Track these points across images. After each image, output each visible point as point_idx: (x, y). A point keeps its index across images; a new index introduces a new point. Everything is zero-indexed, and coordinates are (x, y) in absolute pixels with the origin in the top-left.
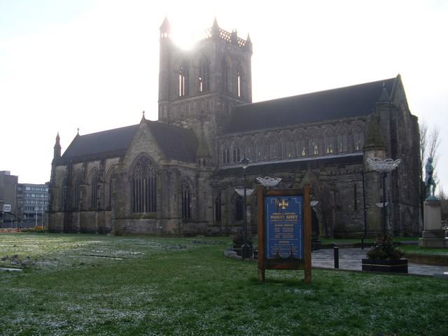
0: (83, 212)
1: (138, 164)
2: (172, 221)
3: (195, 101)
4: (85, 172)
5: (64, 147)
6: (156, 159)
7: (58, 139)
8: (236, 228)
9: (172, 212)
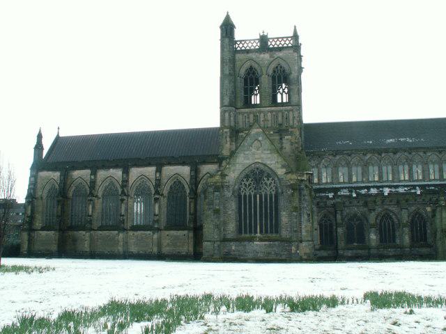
0: (92, 232)
1: (247, 177)
2: (304, 244)
3: (271, 112)
4: (93, 183)
5: (47, 145)
6: (281, 172)
7: (40, 137)
8: (350, 251)
9: (304, 233)
